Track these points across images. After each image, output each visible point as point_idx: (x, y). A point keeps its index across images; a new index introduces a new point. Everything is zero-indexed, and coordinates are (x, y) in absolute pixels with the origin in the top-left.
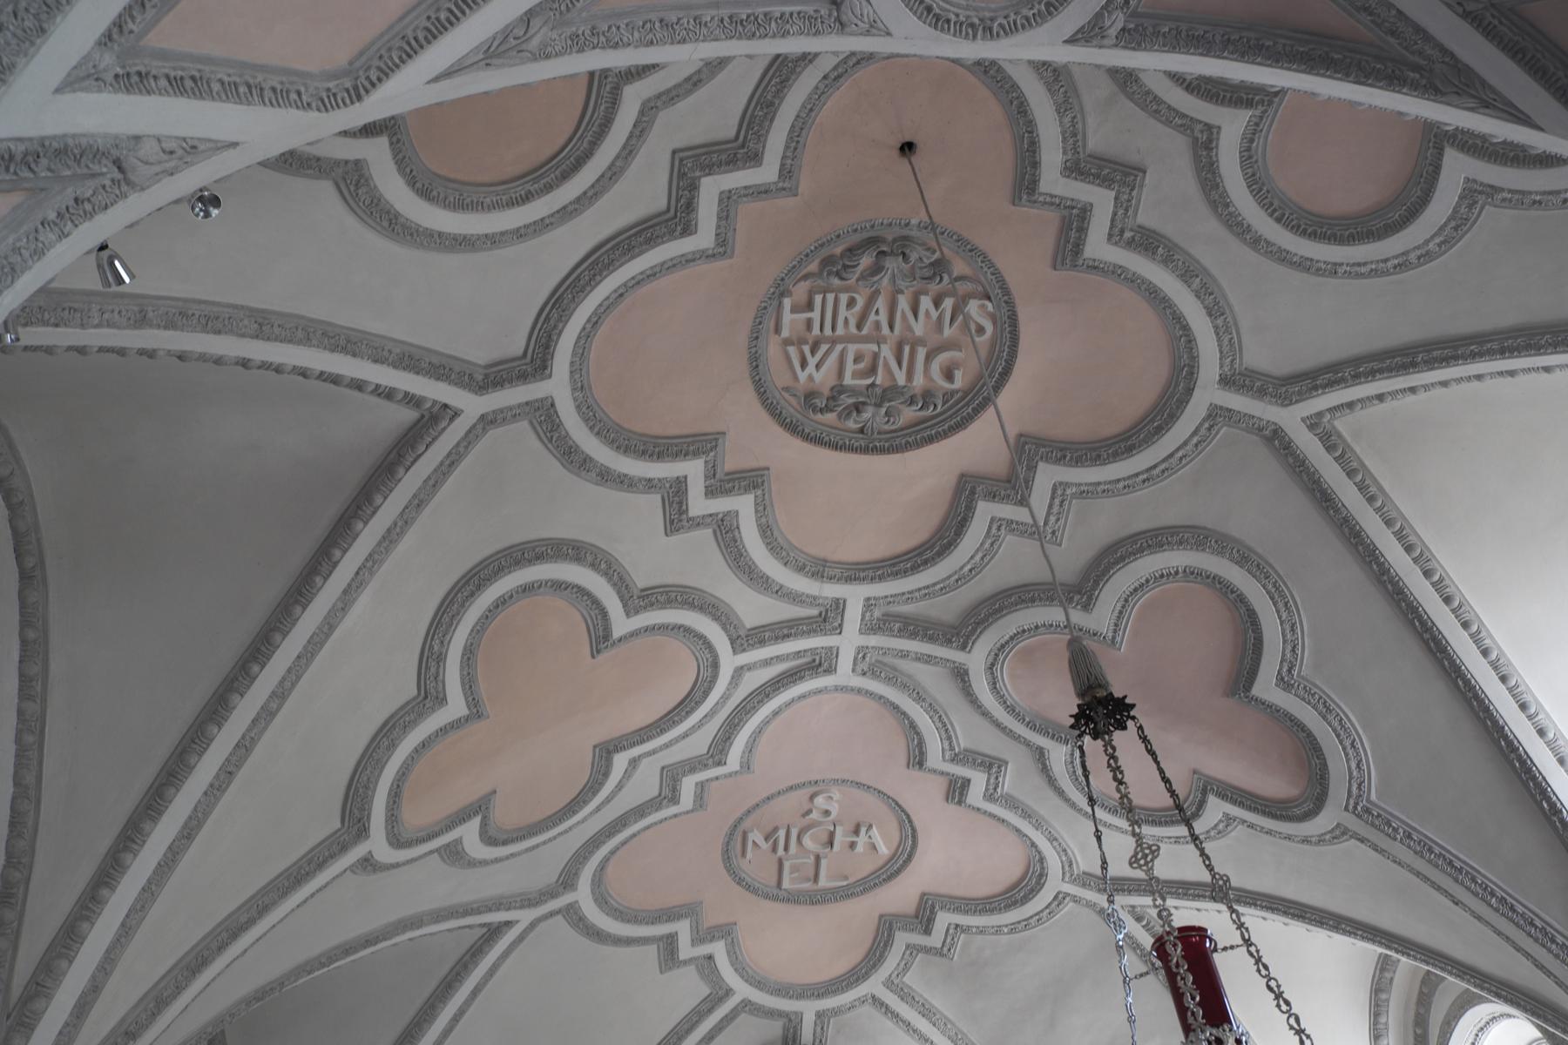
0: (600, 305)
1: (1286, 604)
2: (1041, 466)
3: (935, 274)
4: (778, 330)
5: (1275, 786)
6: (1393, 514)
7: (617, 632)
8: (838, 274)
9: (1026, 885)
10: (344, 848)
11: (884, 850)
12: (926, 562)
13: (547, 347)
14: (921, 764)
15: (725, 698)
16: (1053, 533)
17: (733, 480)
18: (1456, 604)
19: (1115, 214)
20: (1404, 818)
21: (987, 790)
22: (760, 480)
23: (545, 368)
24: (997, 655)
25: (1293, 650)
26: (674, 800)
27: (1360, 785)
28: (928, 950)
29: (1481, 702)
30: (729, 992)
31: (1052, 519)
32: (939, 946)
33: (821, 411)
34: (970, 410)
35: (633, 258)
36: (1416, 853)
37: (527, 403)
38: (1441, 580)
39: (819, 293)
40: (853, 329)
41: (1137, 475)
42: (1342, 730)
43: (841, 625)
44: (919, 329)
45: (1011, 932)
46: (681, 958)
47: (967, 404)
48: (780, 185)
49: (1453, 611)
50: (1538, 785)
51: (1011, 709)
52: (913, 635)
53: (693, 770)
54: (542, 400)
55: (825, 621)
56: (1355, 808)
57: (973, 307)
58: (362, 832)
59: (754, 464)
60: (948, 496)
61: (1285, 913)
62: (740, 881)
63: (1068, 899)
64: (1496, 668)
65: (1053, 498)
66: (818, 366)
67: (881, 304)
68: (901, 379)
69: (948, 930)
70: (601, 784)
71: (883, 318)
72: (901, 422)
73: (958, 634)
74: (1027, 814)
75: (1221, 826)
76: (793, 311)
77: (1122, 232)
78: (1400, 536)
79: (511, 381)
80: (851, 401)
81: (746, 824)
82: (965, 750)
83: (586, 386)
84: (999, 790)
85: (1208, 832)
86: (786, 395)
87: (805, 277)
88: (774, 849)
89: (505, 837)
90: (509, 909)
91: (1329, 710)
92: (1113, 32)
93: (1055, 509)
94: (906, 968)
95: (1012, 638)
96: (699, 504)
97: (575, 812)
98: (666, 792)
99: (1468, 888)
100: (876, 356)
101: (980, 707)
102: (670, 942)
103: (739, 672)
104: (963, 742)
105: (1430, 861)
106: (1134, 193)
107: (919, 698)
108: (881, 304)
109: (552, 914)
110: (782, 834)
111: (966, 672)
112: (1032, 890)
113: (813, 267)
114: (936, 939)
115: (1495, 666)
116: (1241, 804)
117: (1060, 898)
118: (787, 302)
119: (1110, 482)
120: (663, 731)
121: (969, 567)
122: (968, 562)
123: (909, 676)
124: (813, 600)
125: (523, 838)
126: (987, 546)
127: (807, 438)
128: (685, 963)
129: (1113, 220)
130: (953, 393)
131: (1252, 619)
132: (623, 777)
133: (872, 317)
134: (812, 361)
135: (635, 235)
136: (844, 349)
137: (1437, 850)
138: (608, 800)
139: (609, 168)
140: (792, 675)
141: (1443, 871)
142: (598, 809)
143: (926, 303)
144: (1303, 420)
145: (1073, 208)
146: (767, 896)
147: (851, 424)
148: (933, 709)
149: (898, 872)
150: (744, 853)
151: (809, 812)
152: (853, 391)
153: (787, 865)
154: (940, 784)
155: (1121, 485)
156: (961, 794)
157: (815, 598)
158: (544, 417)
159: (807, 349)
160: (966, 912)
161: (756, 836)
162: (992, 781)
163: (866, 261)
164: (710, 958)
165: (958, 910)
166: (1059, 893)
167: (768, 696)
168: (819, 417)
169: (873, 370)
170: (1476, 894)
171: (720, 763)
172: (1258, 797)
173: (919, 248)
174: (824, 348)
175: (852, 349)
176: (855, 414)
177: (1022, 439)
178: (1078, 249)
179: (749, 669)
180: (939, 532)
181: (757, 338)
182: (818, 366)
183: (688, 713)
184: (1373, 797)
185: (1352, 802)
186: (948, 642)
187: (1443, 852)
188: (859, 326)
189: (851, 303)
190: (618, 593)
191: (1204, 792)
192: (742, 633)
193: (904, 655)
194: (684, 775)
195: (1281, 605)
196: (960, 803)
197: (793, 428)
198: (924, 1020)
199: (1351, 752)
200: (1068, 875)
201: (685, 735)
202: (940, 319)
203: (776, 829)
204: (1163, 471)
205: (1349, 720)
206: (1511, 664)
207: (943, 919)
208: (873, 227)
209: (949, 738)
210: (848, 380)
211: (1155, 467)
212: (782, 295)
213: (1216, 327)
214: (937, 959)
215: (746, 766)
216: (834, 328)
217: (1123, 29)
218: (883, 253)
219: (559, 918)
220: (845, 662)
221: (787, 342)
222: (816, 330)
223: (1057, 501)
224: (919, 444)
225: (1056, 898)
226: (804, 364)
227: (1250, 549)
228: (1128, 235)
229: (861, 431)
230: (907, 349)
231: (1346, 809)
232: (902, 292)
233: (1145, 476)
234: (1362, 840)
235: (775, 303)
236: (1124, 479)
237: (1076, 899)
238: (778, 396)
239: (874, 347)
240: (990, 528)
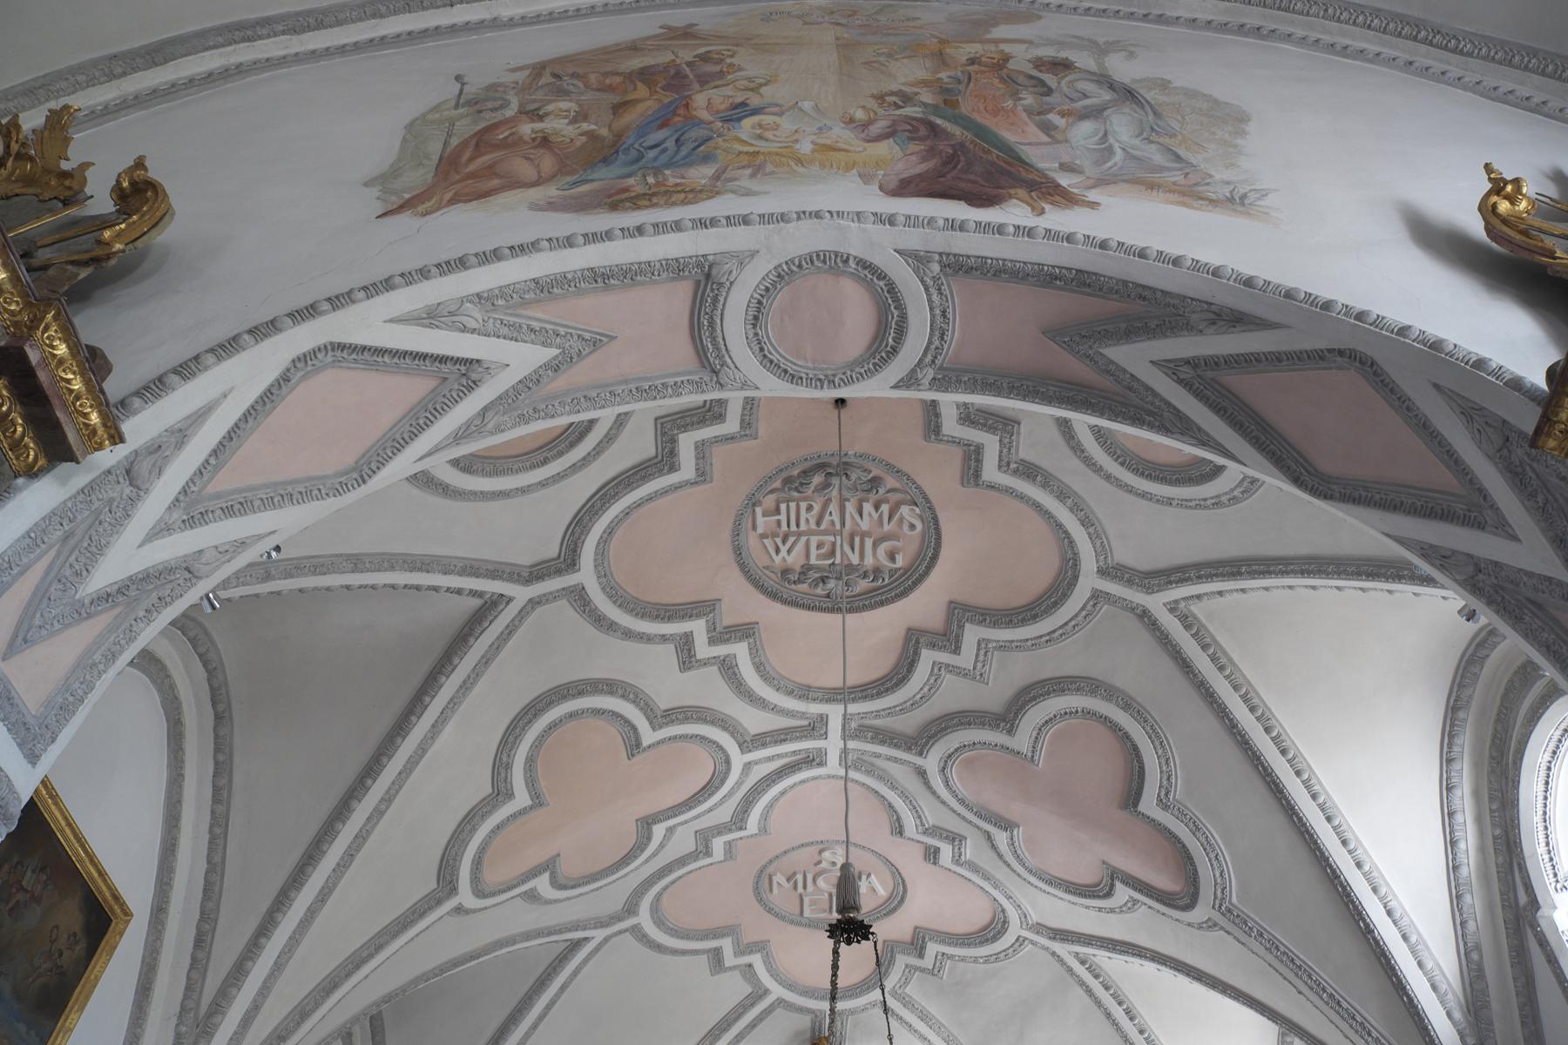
0: (612, 522)
1: (1161, 743)
2: (968, 626)
3: (872, 488)
4: (754, 528)
5: (1164, 882)
6: (1241, 680)
7: (645, 743)
8: (797, 490)
9: (994, 928)
10: (439, 902)
11: (882, 892)
12: (887, 690)
13: (575, 551)
14: (901, 833)
15: (739, 784)
16: (981, 675)
17: (730, 632)
18: (1290, 756)
19: (1001, 452)
20: (1257, 919)
21: (953, 857)
22: (751, 632)
23: (575, 565)
24: (946, 762)
25: (1168, 779)
26: (708, 853)
27: (1223, 890)
28: (923, 970)
29: (1311, 836)
30: (767, 992)
31: (979, 665)
32: (931, 968)
33: (794, 582)
34: (910, 583)
35: (632, 490)
36: (1266, 949)
37: (563, 589)
38: (1279, 735)
39: (784, 502)
40: (813, 526)
41: (1041, 637)
42: (1208, 846)
43: (826, 733)
44: (865, 525)
45: (986, 962)
46: (727, 965)
47: (908, 579)
48: (743, 433)
49: (1289, 761)
50: (1356, 908)
51: (962, 801)
52: (882, 742)
53: (720, 833)
54: (574, 586)
55: (813, 729)
56: (1220, 907)
57: (905, 510)
58: (453, 890)
59: (747, 620)
60: (900, 644)
61: (1188, 975)
62: (770, 911)
63: (1026, 942)
64: (1323, 810)
65: (978, 650)
66: (789, 552)
67: (833, 507)
68: (855, 560)
69: (936, 957)
70: (646, 845)
71: (836, 518)
72: (858, 590)
73: (916, 744)
74: (986, 877)
75: (1129, 905)
76: (764, 515)
77: (1008, 464)
78: (1246, 699)
79: (549, 575)
80: (817, 575)
81: (770, 869)
82: (934, 826)
83: (608, 573)
84: (963, 857)
85: (1121, 907)
86: (767, 572)
87: (772, 492)
88: (795, 888)
89: (572, 883)
90: (584, 929)
91: (1198, 828)
92: (926, 382)
93: (981, 658)
94: (906, 983)
95: (956, 750)
96: (703, 650)
97: (628, 864)
98: (701, 848)
99: (1306, 983)
100: (834, 544)
101: (939, 797)
102: (717, 954)
103: (747, 767)
104: (931, 820)
105: (1277, 957)
106: (1014, 438)
107: (893, 787)
108: (833, 507)
109: (620, 932)
110: (800, 877)
111: (925, 772)
112: (999, 932)
113: (777, 484)
114: (928, 962)
115: (1322, 807)
116: (1140, 891)
117: (1020, 941)
118: (759, 510)
119: (1020, 641)
120: (691, 808)
121: (920, 696)
122: (919, 692)
123: (883, 770)
124: (803, 715)
125: (588, 883)
126: (932, 681)
127: (785, 602)
128: (730, 969)
129: (1000, 456)
130: (897, 570)
131: (1135, 753)
132: (664, 839)
133: (827, 517)
134: (784, 549)
135: (632, 474)
136: (808, 539)
137: (1282, 948)
138: (654, 855)
139: (606, 436)
140: (792, 767)
141: (1286, 966)
142: (647, 861)
143: (868, 507)
144: (1165, 605)
145: (970, 445)
146: (792, 922)
147: (819, 591)
148: (904, 795)
149: (894, 910)
150: (771, 890)
151: (819, 862)
152: (818, 569)
153: (806, 900)
154: (918, 852)
155: (1029, 643)
156: (935, 858)
157: (803, 713)
158: (579, 597)
159: (779, 541)
160: (949, 944)
161: (779, 878)
162: (956, 850)
163: (817, 479)
164: (750, 966)
165: (943, 942)
166: (1019, 937)
167: (774, 781)
168: (793, 586)
169: (832, 553)
170: (1312, 989)
171: (741, 829)
172: (1152, 887)
173: (858, 471)
174: (792, 539)
175: (814, 540)
176: (821, 585)
177: (953, 605)
178: (977, 474)
179: (756, 764)
180: (895, 669)
181: (738, 535)
182: (789, 552)
183: (710, 795)
184: (1234, 900)
185: (1217, 902)
186: (909, 749)
188: (818, 523)
189: (810, 508)
191: (1113, 880)
192: (748, 739)
193: (878, 756)
194: (713, 837)
195: (1157, 743)
196: (935, 863)
197: (774, 595)
198: (922, 1023)
199: (1215, 863)
200: (1025, 924)
201: (710, 810)
202: (881, 517)
203: (795, 874)
204: (1061, 635)
205: (1214, 838)
206: (1337, 807)
207: (932, 949)
208: (819, 456)
209: (920, 817)
210: (813, 561)
211: (1054, 631)
212: (754, 505)
213: (1089, 534)
214: (930, 977)
215: (763, 830)
216: (798, 526)
217: (934, 379)
218: (830, 474)
219: (628, 934)
220: (833, 758)
221: (763, 536)
222: (784, 527)
223: (982, 652)
224: (873, 607)
225: (1017, 940)
226: (778, 551)
227: (1131, 698)
228: (1013, 466)
229: (828, 596)
230: (857, 540)
231: (1214, 907)
232: (848, 500)
233: (1047, 638)
234: (1229, 933)
235: (750, 510)
236: (1032, 639)
237: (1033, 943)
238: (759, 572)
239: (832, 539)
240: (932, 669)
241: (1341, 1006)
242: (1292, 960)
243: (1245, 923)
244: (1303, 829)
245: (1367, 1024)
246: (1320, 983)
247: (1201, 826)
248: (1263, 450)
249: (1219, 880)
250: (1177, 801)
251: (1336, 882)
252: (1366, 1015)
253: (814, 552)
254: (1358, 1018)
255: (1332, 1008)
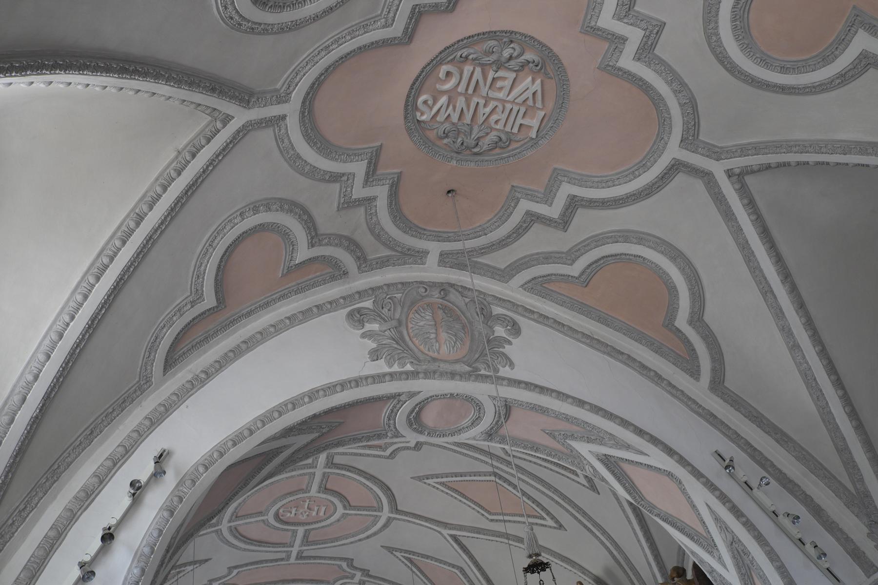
54: (687, 149)
67: (481, 119)
71: (481, 110)
76: (530, 127)
96: (635, 36)
108: (481, 119)
134: (529, 94)
143: (455, 118)
144: (233, 118)
158: (690, 140)
159: (530, 102)
174: (520, 100)
190: (717, 15)
213: (293, 148)
222: (523, 110)
253: (507, 84)
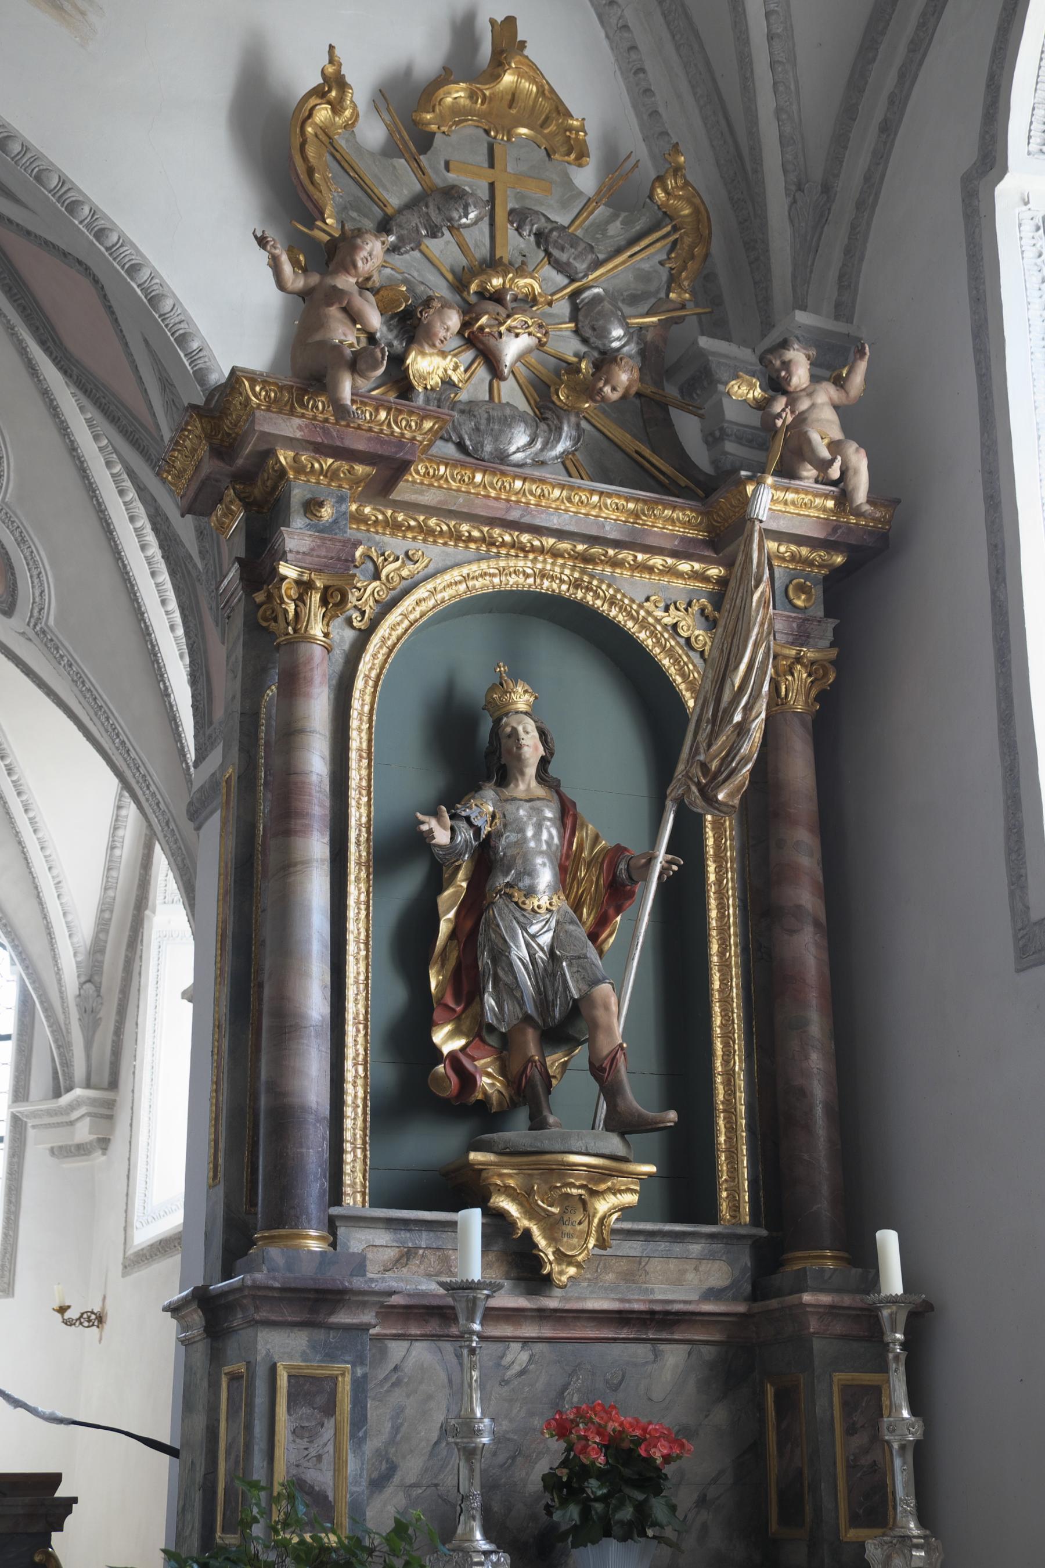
20: (70, 649)
36: (73, 680)
42: (32, 562)
49: (125, 504)
64: (149, 564)
105: (81, 692)
137: (88, 685)
184: (51, 622)
185: (33, 621)
187: (92, 689)
199: (36, 581)
231: (28, 624)
241: (129, 755)
242: (95, 699)
243: (57, 649)
244: (126, 577)
245: (148, 778)
246: (115, 728)
247: (27, 538)
248: (15, 301)
249: (37, 600)
250: (6, 504)
251: (147, 638)
252: (151, 770)
254: (142, 770)
255: (121, 754)
